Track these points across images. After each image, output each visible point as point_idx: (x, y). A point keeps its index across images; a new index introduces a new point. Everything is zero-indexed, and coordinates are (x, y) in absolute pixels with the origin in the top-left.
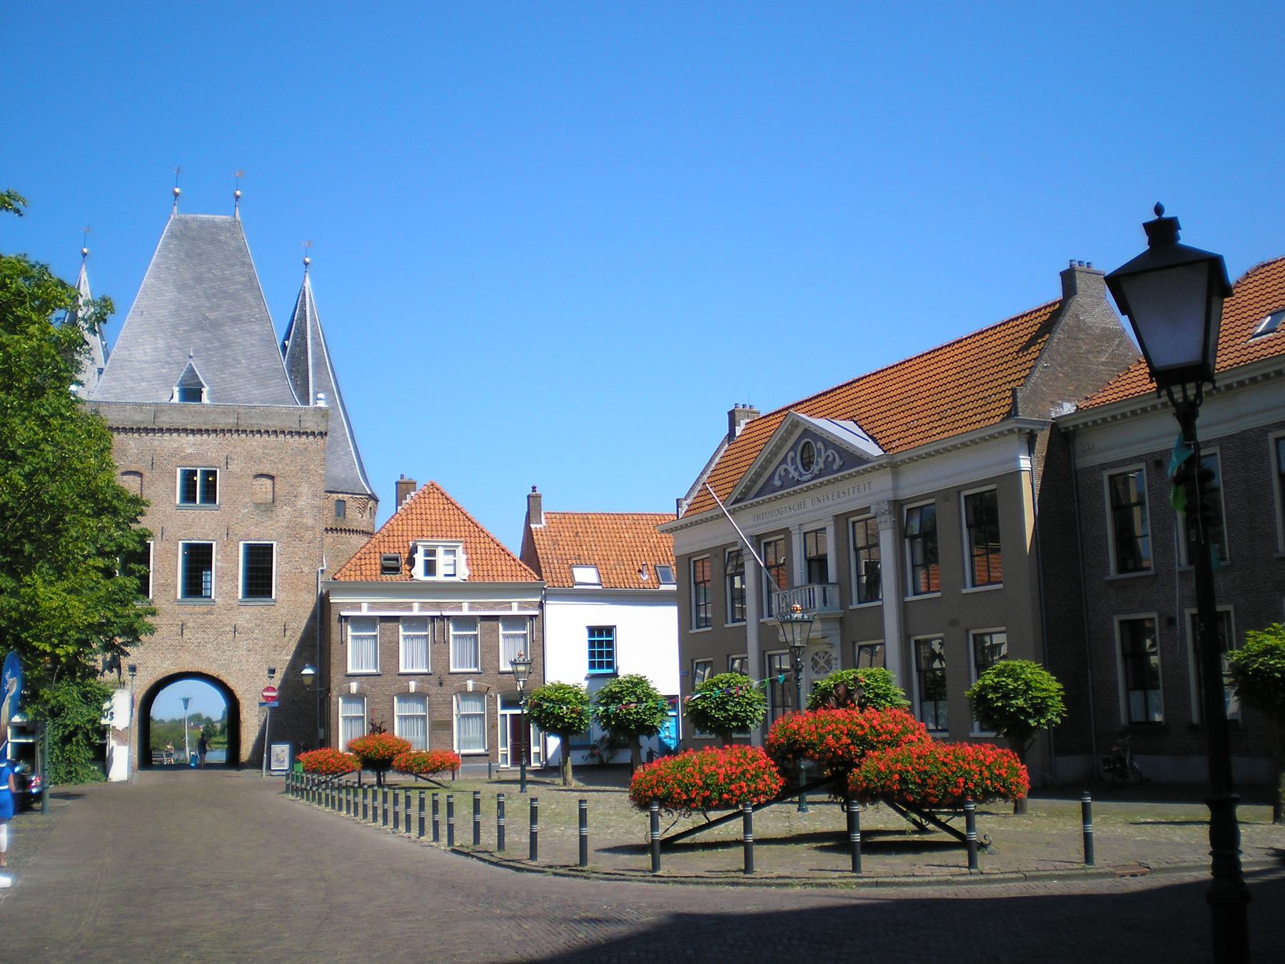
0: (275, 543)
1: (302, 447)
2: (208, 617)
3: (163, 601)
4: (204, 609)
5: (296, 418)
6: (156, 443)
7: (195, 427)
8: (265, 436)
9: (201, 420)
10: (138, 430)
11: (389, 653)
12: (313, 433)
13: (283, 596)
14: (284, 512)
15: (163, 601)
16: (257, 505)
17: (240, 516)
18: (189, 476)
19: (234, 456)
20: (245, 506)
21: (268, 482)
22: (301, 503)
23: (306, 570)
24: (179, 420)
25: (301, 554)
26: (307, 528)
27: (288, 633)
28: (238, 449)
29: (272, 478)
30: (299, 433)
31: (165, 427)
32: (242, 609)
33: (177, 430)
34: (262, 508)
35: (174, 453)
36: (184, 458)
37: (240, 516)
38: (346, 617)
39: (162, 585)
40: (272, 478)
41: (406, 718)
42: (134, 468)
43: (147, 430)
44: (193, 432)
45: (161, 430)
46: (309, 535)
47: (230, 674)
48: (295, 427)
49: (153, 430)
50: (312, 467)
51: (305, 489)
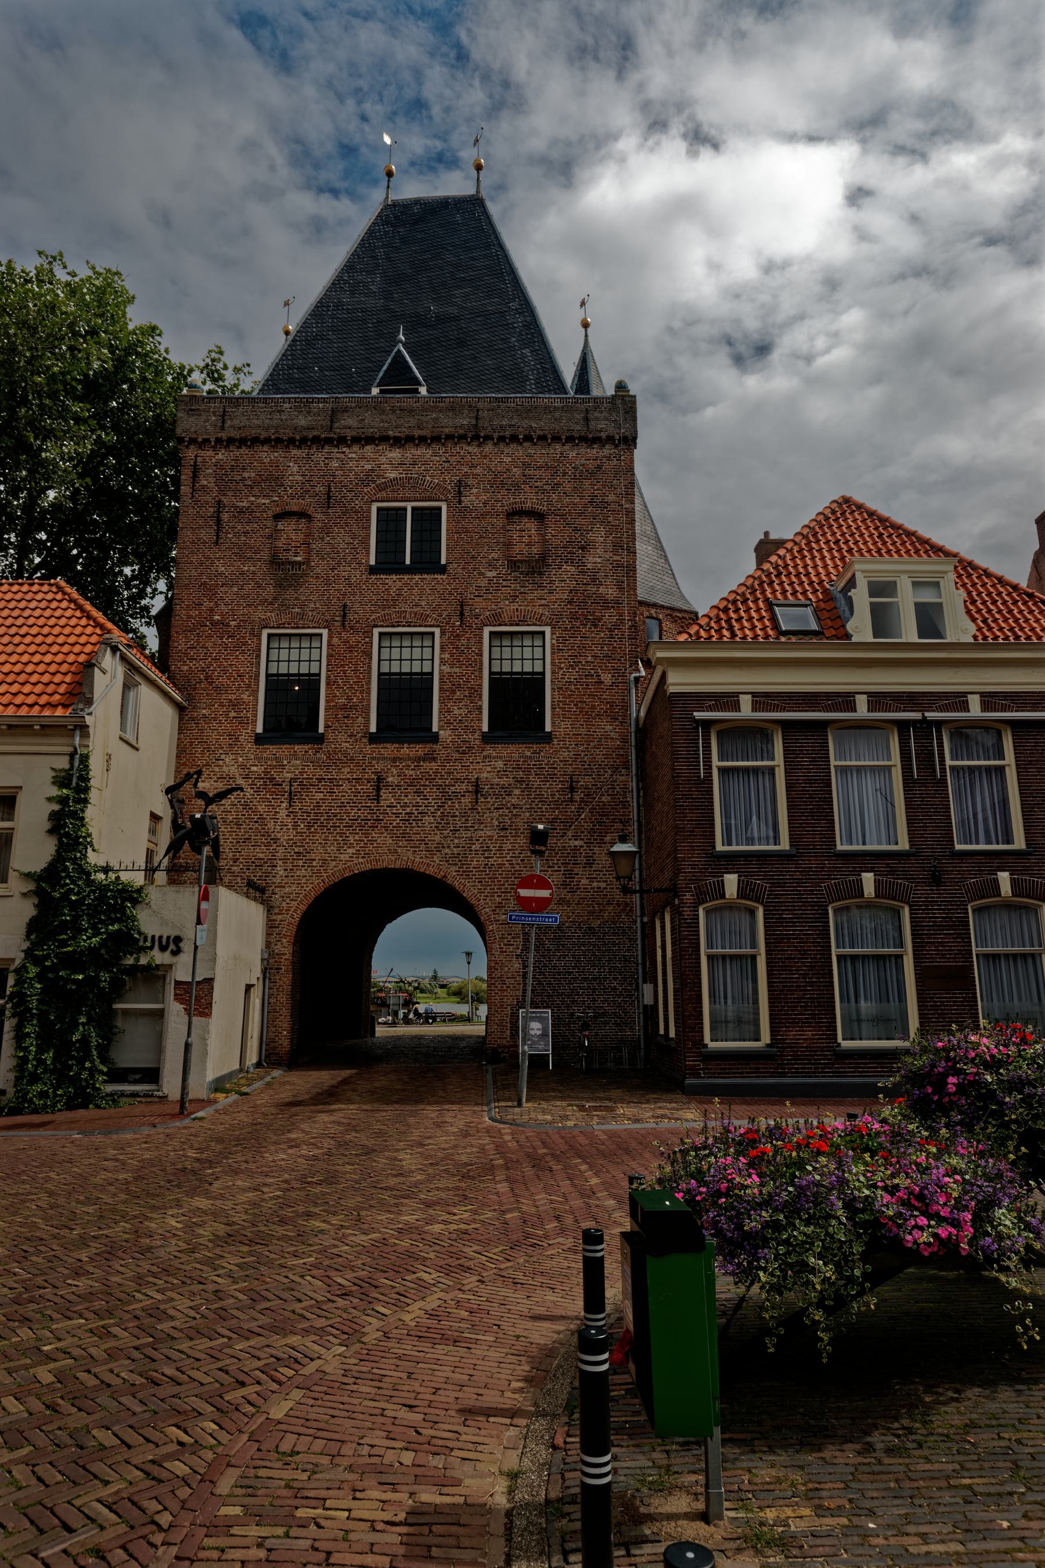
0: (548, 630)
1: (591, 465)
2: (427, 765)
3: (342, 737)
4: (419, 750)
5: (579, 416)
6: (335, 464)
7: (404, 432)
8: (527, 444)
9: (413, 422)
10: (303, 442)
11: (812, 803)
12: (610, 439)
13: (565, 726)
14: (563, 577)
15: (342, 737)
16: (513, 564)
17: (483, 583)
18: (391, 520)
19: (471, 481)
20: (491, 565)
21: (531, 526)
22: (593, 560)
23: (607, 678)
24: (373, 423)
25: (597, 651)
26: (606, 604)
27: (577, 797)
28: (478, 470)
29: (539, 516)
30: (583, 439)
31: (349, 434)
32: (489, 750)
33: (370, 440)
34: (523, 568)
35: (368, 478)
36: (381, 488)
37: (483, 583)
38: (707, 724)
39: (344, 707)
40: (539, 516)
41: (987, 956)
42: (294, 506)
43: (318, 442)
44: (398, 442)
45: (342, 441)
46: (609, 617)
47: (467, 874)
48: (578, 428)
49: (329, 441)
50: (611, 498)
51: (599, 535)
